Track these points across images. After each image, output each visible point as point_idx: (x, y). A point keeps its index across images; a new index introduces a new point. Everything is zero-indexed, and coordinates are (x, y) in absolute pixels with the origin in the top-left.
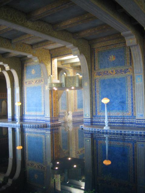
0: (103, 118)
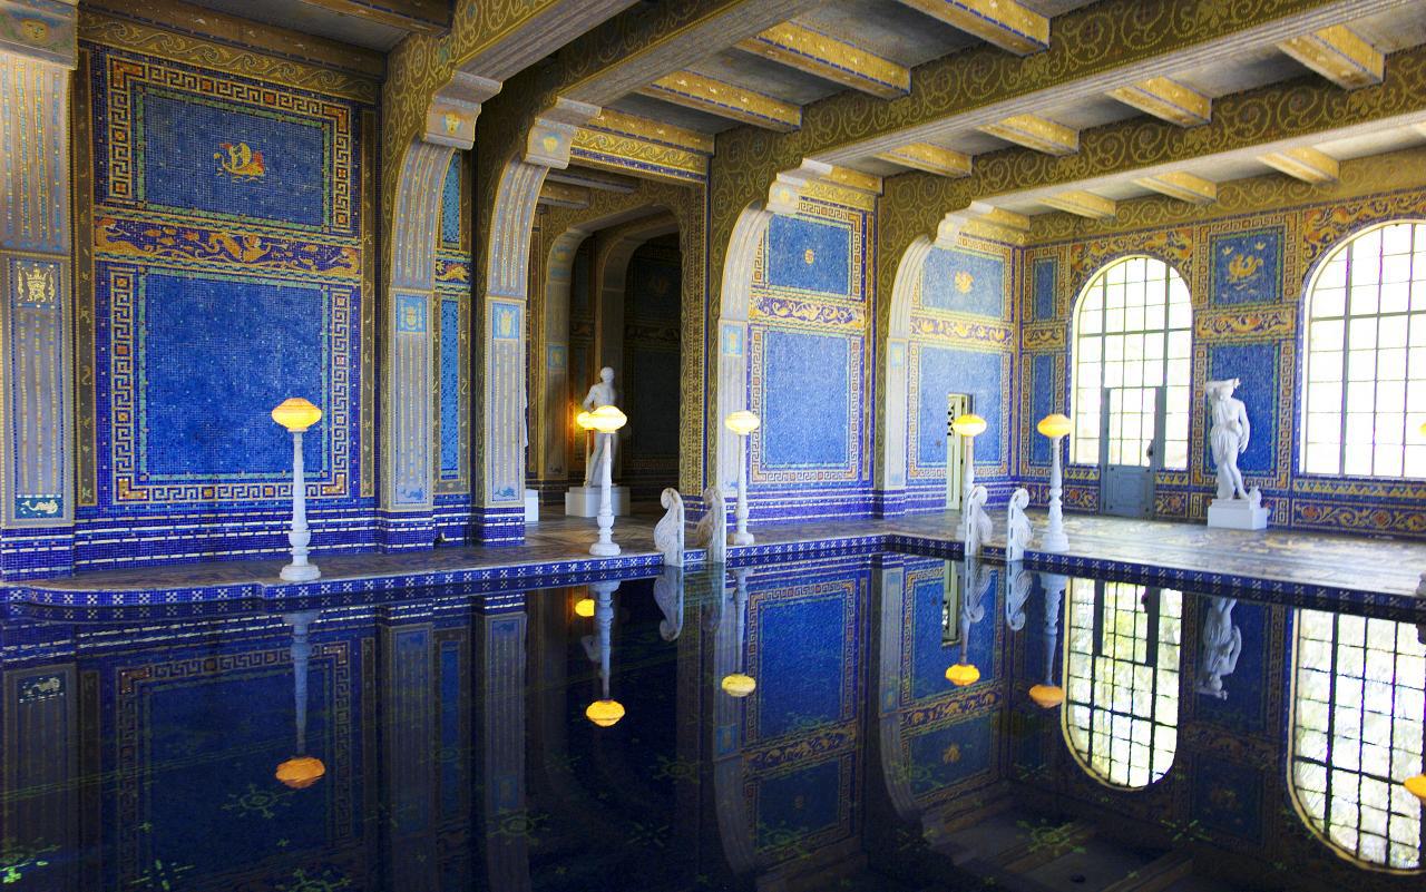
0: (156, 523)
